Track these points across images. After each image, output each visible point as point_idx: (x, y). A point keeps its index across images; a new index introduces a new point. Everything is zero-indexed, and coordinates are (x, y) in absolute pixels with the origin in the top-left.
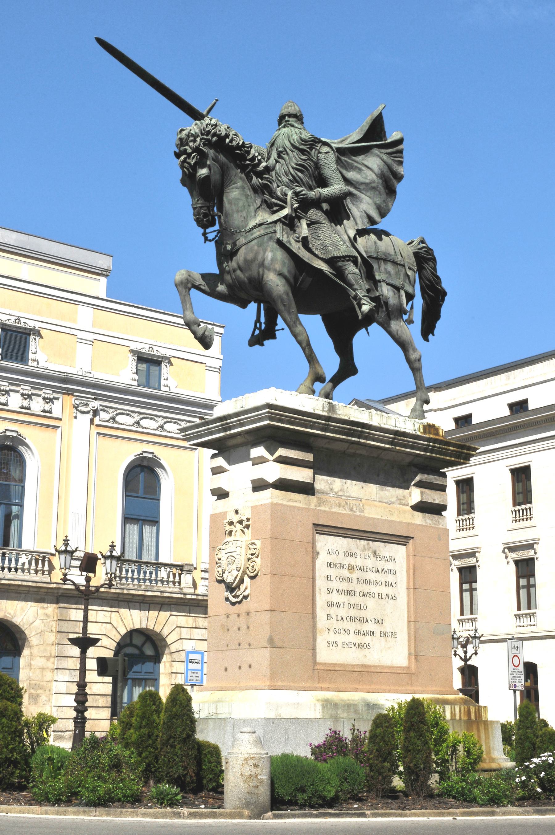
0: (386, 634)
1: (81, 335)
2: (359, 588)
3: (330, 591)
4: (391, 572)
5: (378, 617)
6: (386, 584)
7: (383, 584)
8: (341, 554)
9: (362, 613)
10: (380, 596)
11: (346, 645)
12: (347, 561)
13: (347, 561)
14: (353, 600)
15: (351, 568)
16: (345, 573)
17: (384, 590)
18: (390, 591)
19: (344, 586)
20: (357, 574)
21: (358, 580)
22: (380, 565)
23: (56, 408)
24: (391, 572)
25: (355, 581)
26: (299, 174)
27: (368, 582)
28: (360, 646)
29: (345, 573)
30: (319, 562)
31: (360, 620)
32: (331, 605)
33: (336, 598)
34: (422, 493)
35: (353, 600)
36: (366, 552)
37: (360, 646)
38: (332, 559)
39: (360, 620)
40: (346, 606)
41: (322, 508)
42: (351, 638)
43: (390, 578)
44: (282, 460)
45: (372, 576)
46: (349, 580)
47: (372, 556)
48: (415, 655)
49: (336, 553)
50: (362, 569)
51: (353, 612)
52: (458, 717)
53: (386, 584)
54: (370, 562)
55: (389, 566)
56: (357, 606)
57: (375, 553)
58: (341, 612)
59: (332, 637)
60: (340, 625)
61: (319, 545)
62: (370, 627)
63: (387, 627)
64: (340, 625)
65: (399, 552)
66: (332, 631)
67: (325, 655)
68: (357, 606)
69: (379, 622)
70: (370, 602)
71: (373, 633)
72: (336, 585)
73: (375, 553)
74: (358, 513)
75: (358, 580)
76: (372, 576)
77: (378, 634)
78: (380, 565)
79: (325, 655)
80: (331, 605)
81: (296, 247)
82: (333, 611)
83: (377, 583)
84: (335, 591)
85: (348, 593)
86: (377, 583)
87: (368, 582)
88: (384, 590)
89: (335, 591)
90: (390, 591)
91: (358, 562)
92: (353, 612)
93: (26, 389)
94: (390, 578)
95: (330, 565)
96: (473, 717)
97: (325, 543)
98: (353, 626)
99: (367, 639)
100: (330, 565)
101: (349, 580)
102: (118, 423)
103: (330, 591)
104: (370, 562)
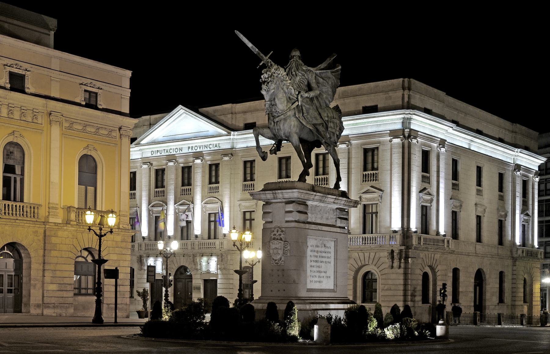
0: (327, 277)
2: (320, 259)
5: (325, 270)
9: (320, 269)
11: (316, 282)
12: (317, 249)
13: (317, 249)
14: (318, 264)
15: (317, 252)
20: (319, 254)
27: (323, 257)
28: (320, 282)
29: (316, 254)
31: (320, 272)
32: (311, 266)
37: (320, 282)
39: (320, 272)
42: (317, 279)
45: (324, 255)
46: (317, 257)
48: (336, 285)
50: (321, 252)
51: (318, 269)
54: (323, 249)
56: (319, 267)
62: (323, 274)
63: (328, 274)
68: (319, 267)
69: (325, 272)
76: (324, 255)
80: (311, 266)
85: (316, 261)
87: (323, 257)
92: (318, 269)
95: (311, 251)
98: (317, 274)
99: (322, 279)
101: (317, 257)
103: (311, 261)
104: (323, 249)
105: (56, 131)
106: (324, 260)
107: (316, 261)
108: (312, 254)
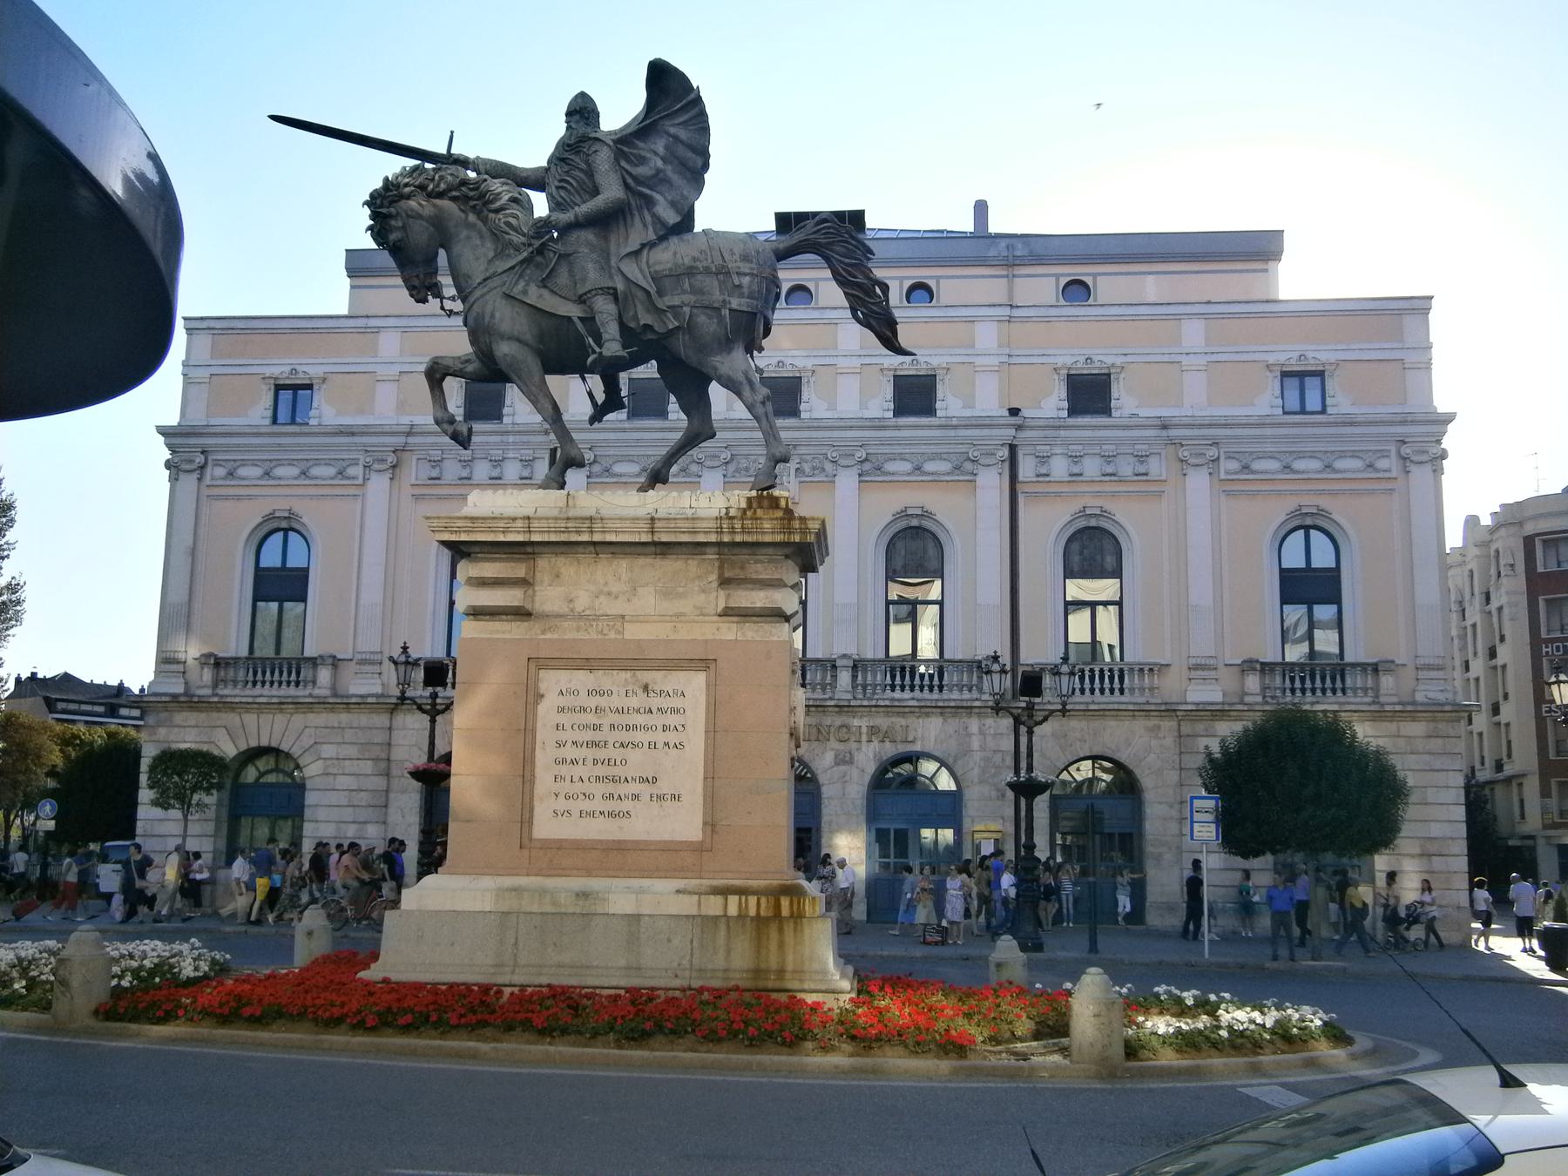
0: (661, 798)
1: (1185, 360)
2: (613, 737)
3: (560, 744)
4: (676, 711)
6: (665, 728)
7: (660, 728)
8: (583, 693)
10: (653, 745)
11: (591, 814)
12: (593, 702)
13: (593, 702)
14: (601, 754)
16: (590, 718)
17: (660, 737)
18: (672, 737)
19: (589, 735)
21: (612, 727)
22: (656, 702)
23: (1155, 467)
24: (676, 711)
25: (606, 728)
26: (562, 193)
30: (542, 708)
33: (570, 752)
34: (728, 597)
35: (601, 754)
36: (630, 688)
38: (562, 701)
40: (589, 762)
41: (549, 636)
42: (597, 805)
43: (673, 720)
44: (482, 583)
45: (640, 719)
47: (640, 691)
48: (710, 825)
49: (576, 693)
51: (601, 770)
52: (752, 912)
53: (665, 728)
54: (634, 702)
55: (676, 702)
57: (646, 688)
58: (578, 771)
59: (561, 805)
60: (578, 788)
61: (543, 687)
62: (634, 788)
63: (664, 787)
64: (578, 788)
65: (695, 684)
66: (561, 797)
67: (545, 827)
70: (634, 756)
71: (636, 797)
72: (568, 735)
73: (646, 688)
74: (612, 635)
75: (612, 727)
76: (640, 719)
77: (645, 797)
78: (656, 702)
79: (545, 827)
81: (535, 295)
82: (564, 770)
83: (646, 728)
84: (569, 744)
85: (595, 744)
86: (646, 728)
88: (660, 737)
89: (569, 744)
90: (672, 737)
91: (616, 701)
92: (601, 770)
93: (1109, 449)
94: (673, 720)
95: (561, 710)
96: (785, 912)
97: (552, 682)
98: (599, 789)
99: (626, 805)
100: (561, 710)
102: (1298, 472)
103: (560, 744)
105: (1198, 483)
106: (639, 736)
107: (595, 744)
108: (564, 719)
